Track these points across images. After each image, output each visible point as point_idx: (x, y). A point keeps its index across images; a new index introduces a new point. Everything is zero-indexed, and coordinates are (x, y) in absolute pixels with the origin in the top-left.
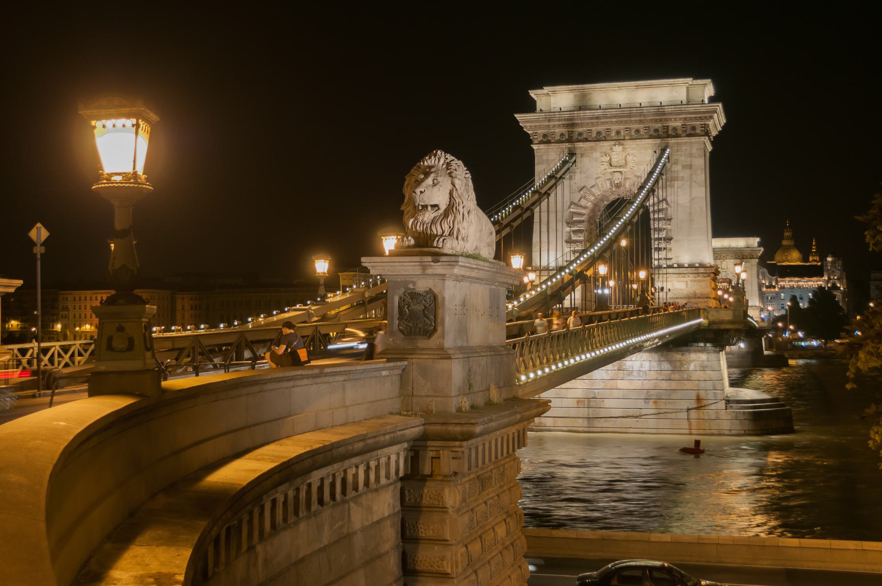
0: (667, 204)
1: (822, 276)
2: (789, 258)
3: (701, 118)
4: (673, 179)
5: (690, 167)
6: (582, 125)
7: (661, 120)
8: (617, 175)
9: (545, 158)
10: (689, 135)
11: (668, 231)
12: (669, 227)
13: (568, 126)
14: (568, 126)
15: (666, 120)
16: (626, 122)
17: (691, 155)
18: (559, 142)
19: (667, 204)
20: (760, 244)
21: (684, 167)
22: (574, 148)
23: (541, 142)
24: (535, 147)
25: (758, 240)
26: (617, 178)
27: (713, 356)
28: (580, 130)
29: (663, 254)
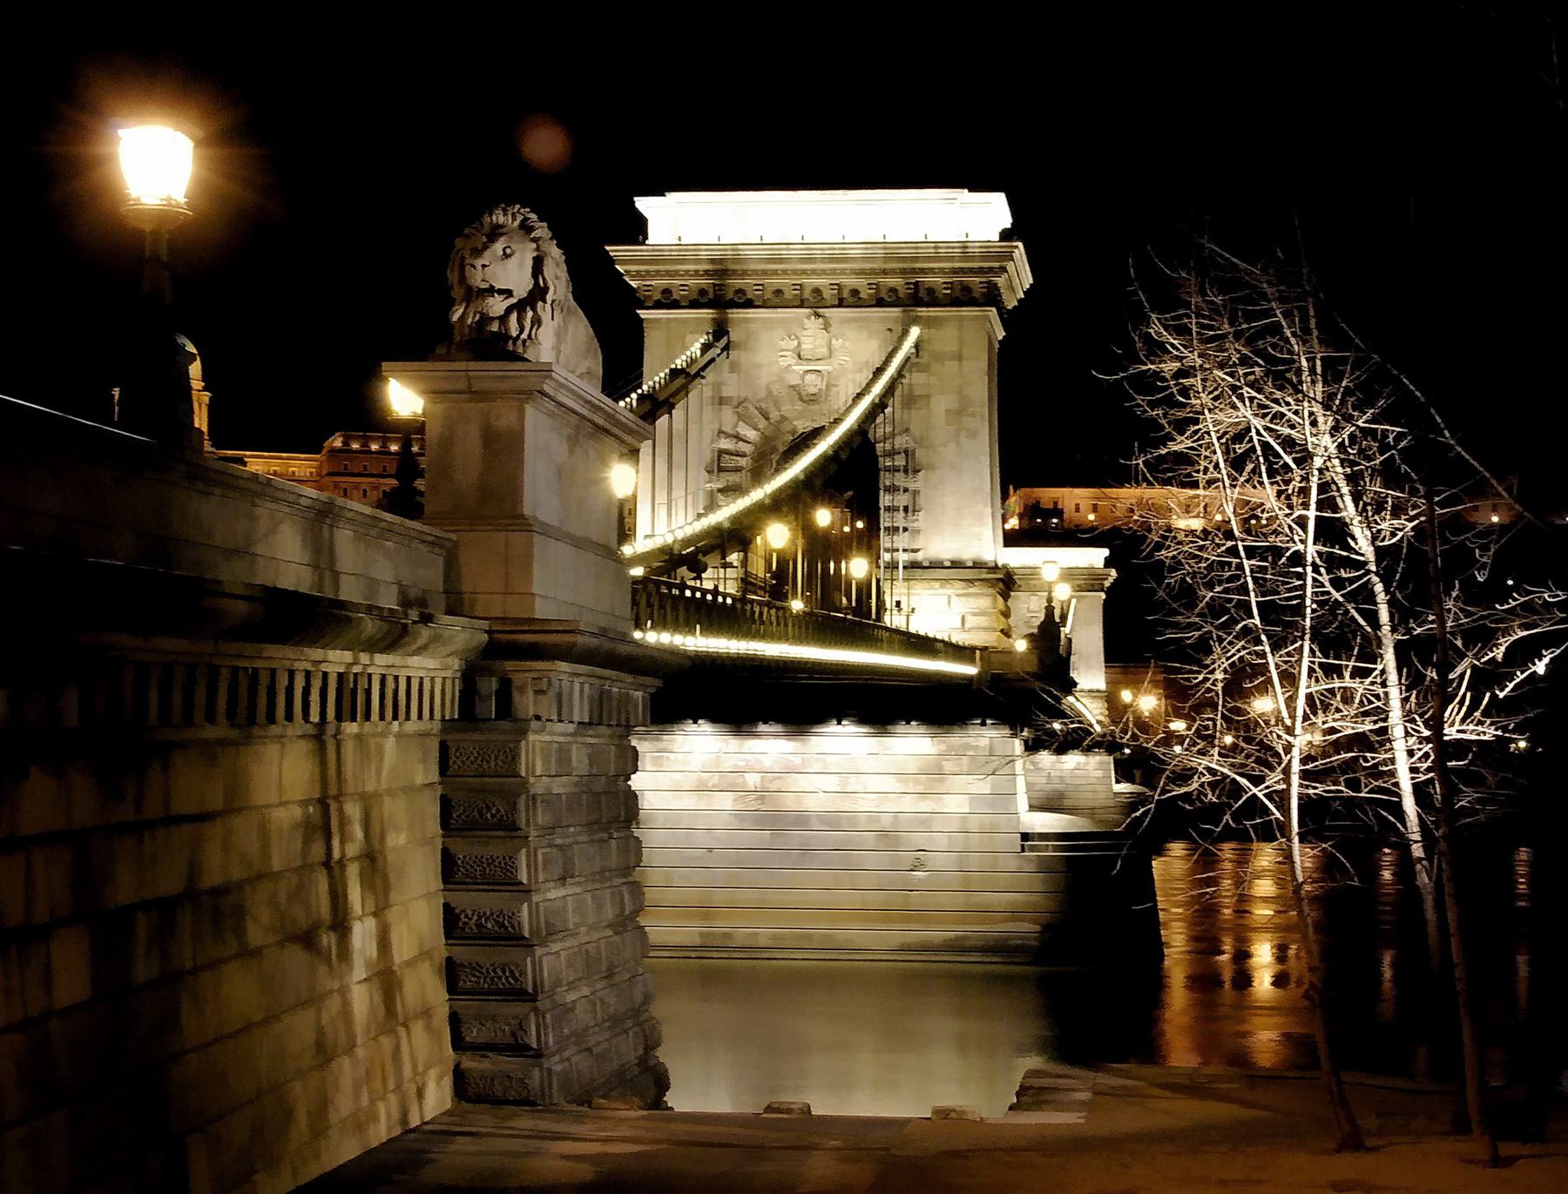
3: (981, 271)
6: (744, 274)
7: (904, 272)
8: (810, 378)
10: (955, 302)
11: (916, 493)
12: (911, 486)
14: (716, 272)
15: (914, 271)
16: (833, 272)
18: (694, 304)
20: (1109, 563)
23: (658, 305)
24: (643, 314)
25: (1106, 552)
26: (813, 384)
28: (737, 283)
29: (901, 541)
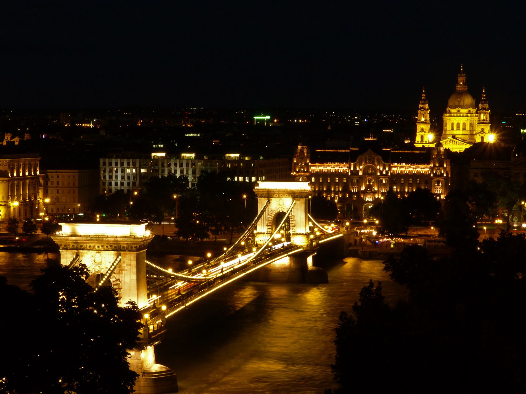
0: (120, 281)
1: (429, 164)
2: (462, 104)
4: (122, 270)
5: (130, 265)
9: (65, 256)
13: (75, 243)
14: (75, 243)
17: (130, 260)
18: (71, 249)
19: (120, 281)
21: (127, 265)
22: (79, 252)
23: (63, 249)
24: (60, 250)
27: (137, 353)
